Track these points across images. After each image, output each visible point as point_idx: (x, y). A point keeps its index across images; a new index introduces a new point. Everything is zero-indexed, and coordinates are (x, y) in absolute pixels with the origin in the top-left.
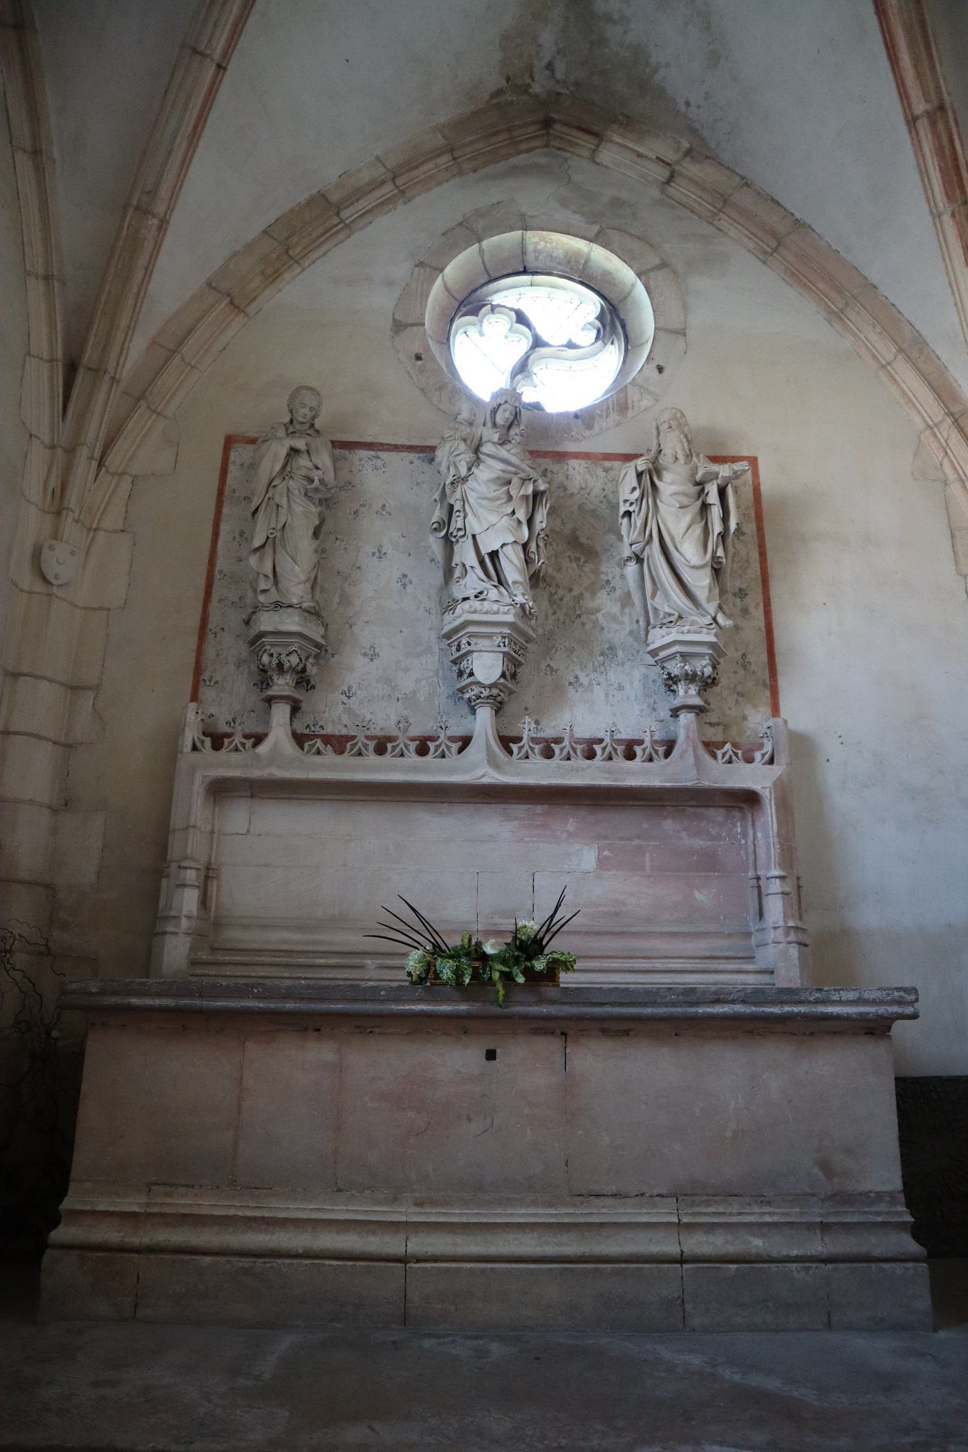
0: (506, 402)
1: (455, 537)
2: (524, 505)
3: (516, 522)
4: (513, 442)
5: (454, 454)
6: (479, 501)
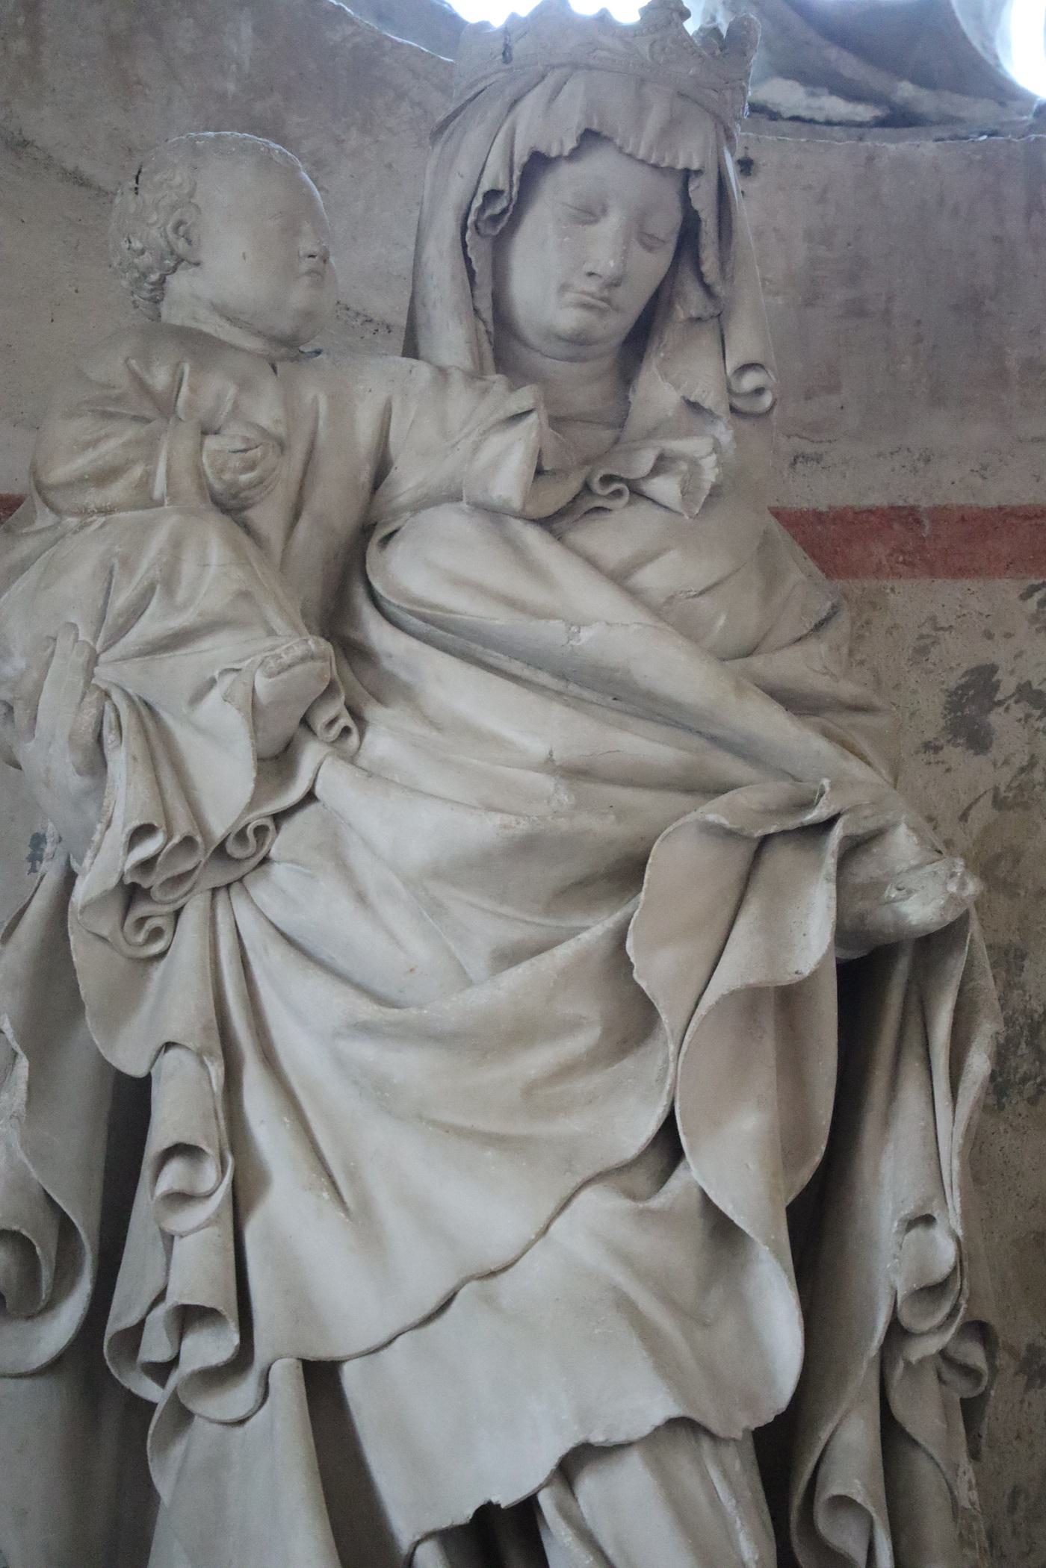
0: (590, 138)
1: (161, 1371)
2: (764, 1077)
3: (697, 1228)
4: (666, 488)
5: (150, 626)
6: (366, 1051)
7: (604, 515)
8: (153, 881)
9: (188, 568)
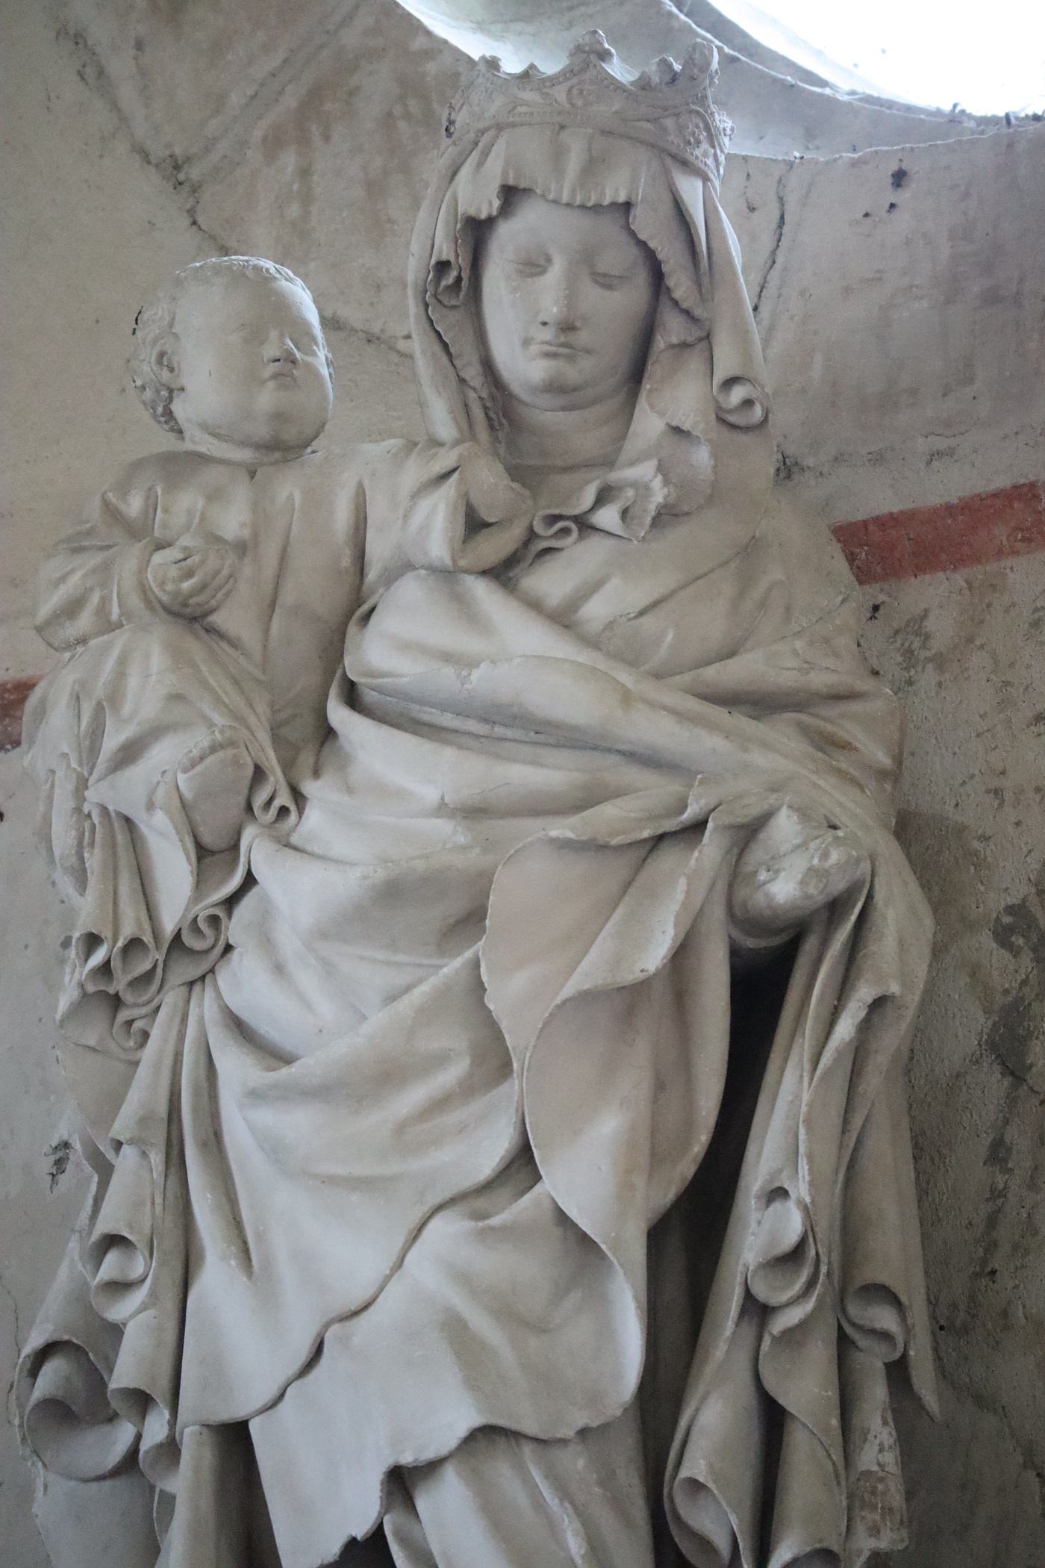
0: (511, 195)
5: (111, 743)
7: (557, 555)
8: (119, 984)
9: (133, 682)
